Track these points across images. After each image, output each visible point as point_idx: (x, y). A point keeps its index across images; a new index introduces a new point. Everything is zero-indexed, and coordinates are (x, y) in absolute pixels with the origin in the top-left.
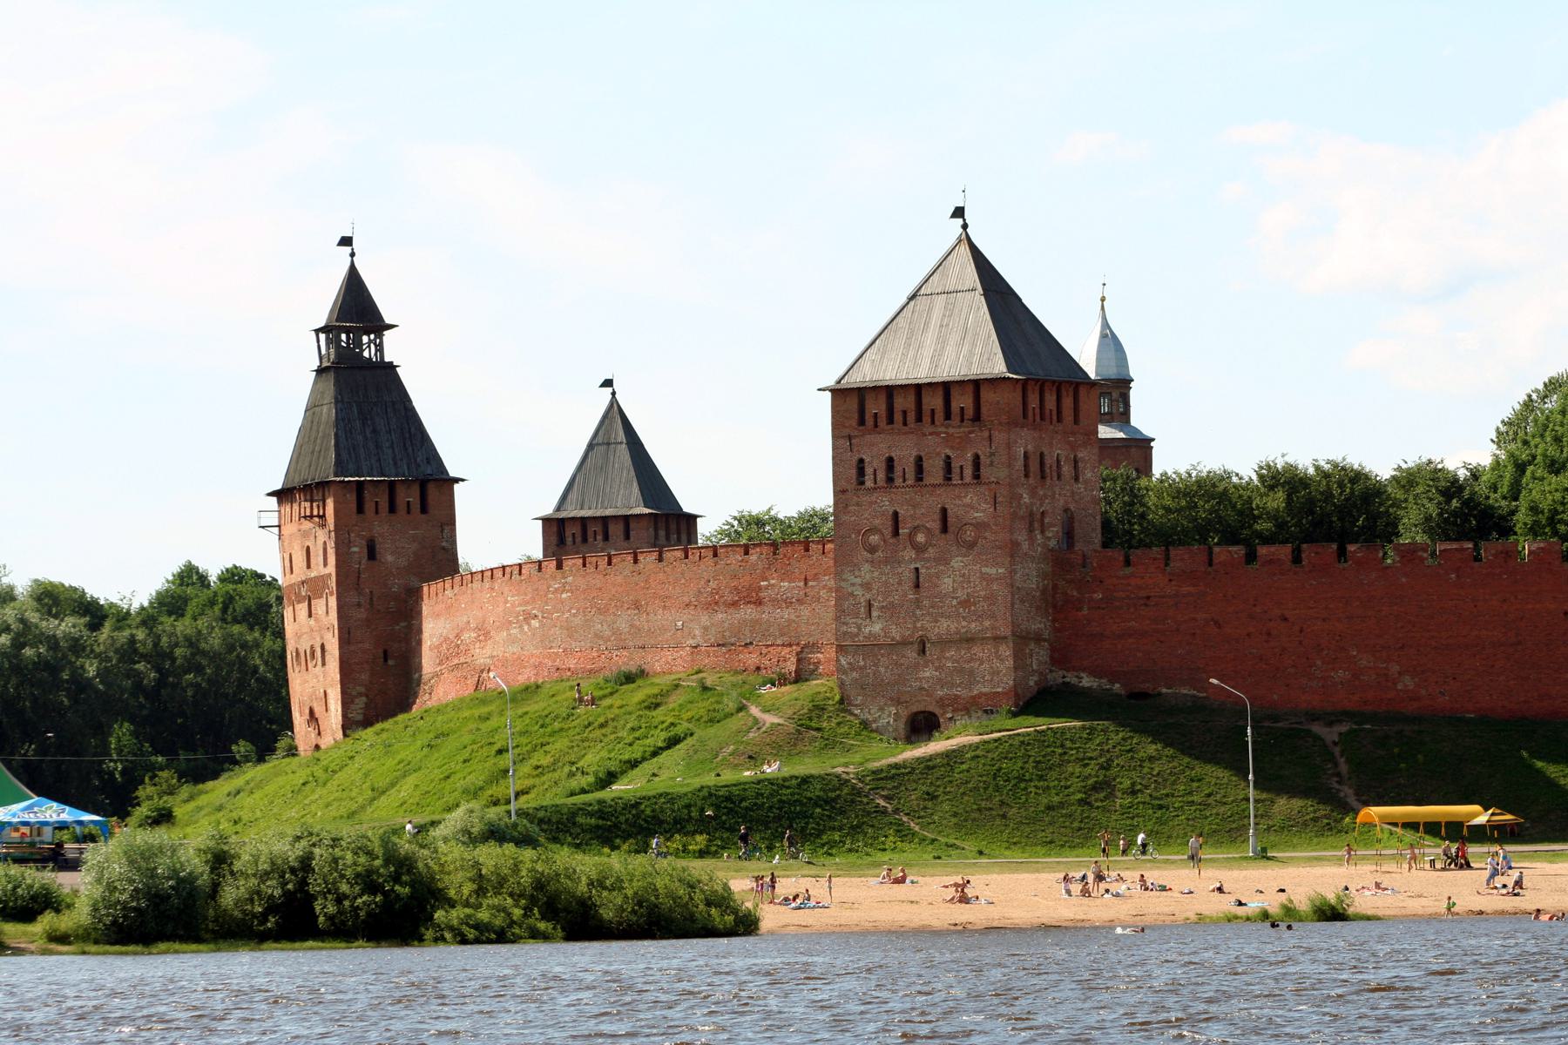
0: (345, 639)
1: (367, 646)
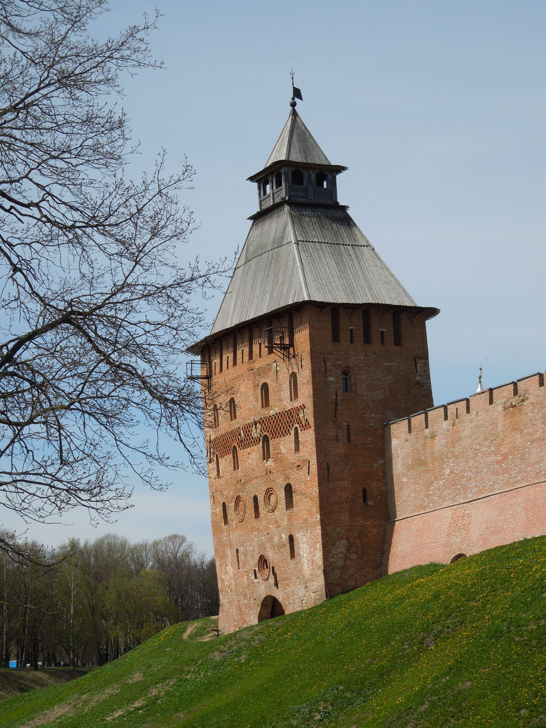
0: (325, 475)
1: (346, 483)
